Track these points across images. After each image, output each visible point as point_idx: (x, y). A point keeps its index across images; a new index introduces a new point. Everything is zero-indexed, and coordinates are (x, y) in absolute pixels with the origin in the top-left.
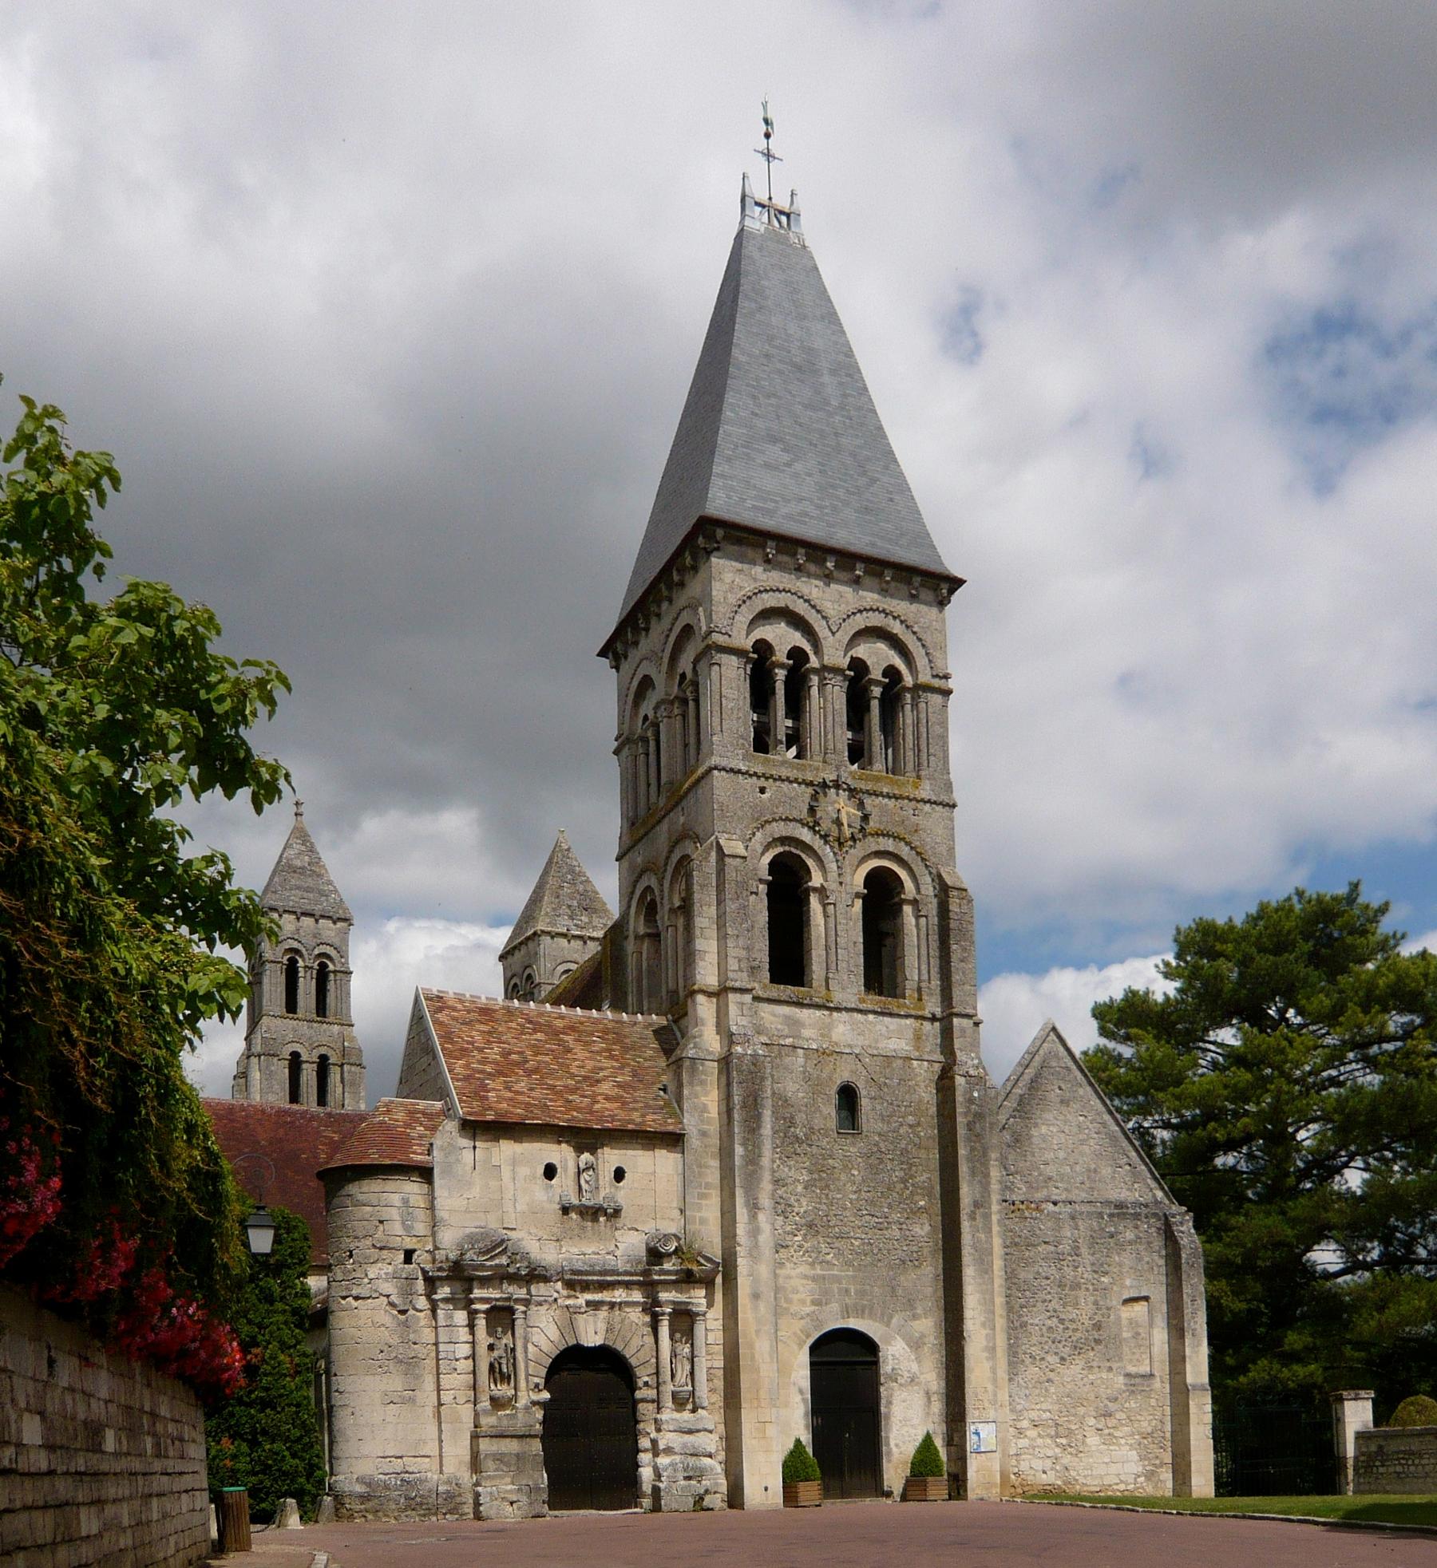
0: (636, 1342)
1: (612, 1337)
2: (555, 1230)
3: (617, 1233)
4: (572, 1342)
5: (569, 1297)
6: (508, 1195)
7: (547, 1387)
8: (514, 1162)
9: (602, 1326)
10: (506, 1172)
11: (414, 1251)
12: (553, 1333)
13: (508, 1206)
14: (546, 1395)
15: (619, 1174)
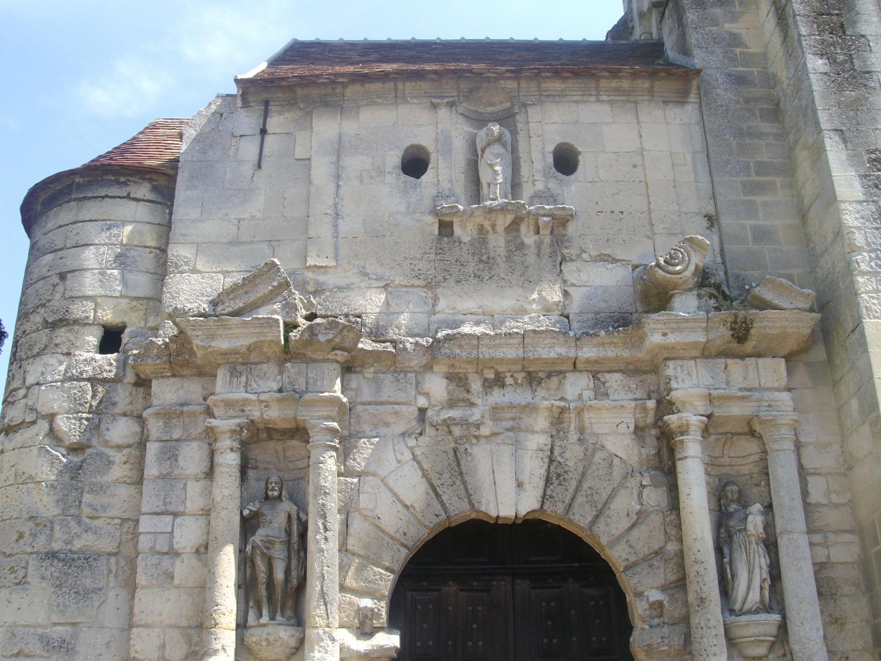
0: (625, 503)
1: (562, 494)
2: (421, 266)
3: (567, 268)
4: (459, 510)
5: (452, 403)
6: (323, 204)
7: (393, 624)
8: (339, 149)
9: (534, 469)
10: (321, 171)
11: (123, 328)
12: (411, 486)
13: (322, 229)
14: (392, 640)
15: (565, 161)
